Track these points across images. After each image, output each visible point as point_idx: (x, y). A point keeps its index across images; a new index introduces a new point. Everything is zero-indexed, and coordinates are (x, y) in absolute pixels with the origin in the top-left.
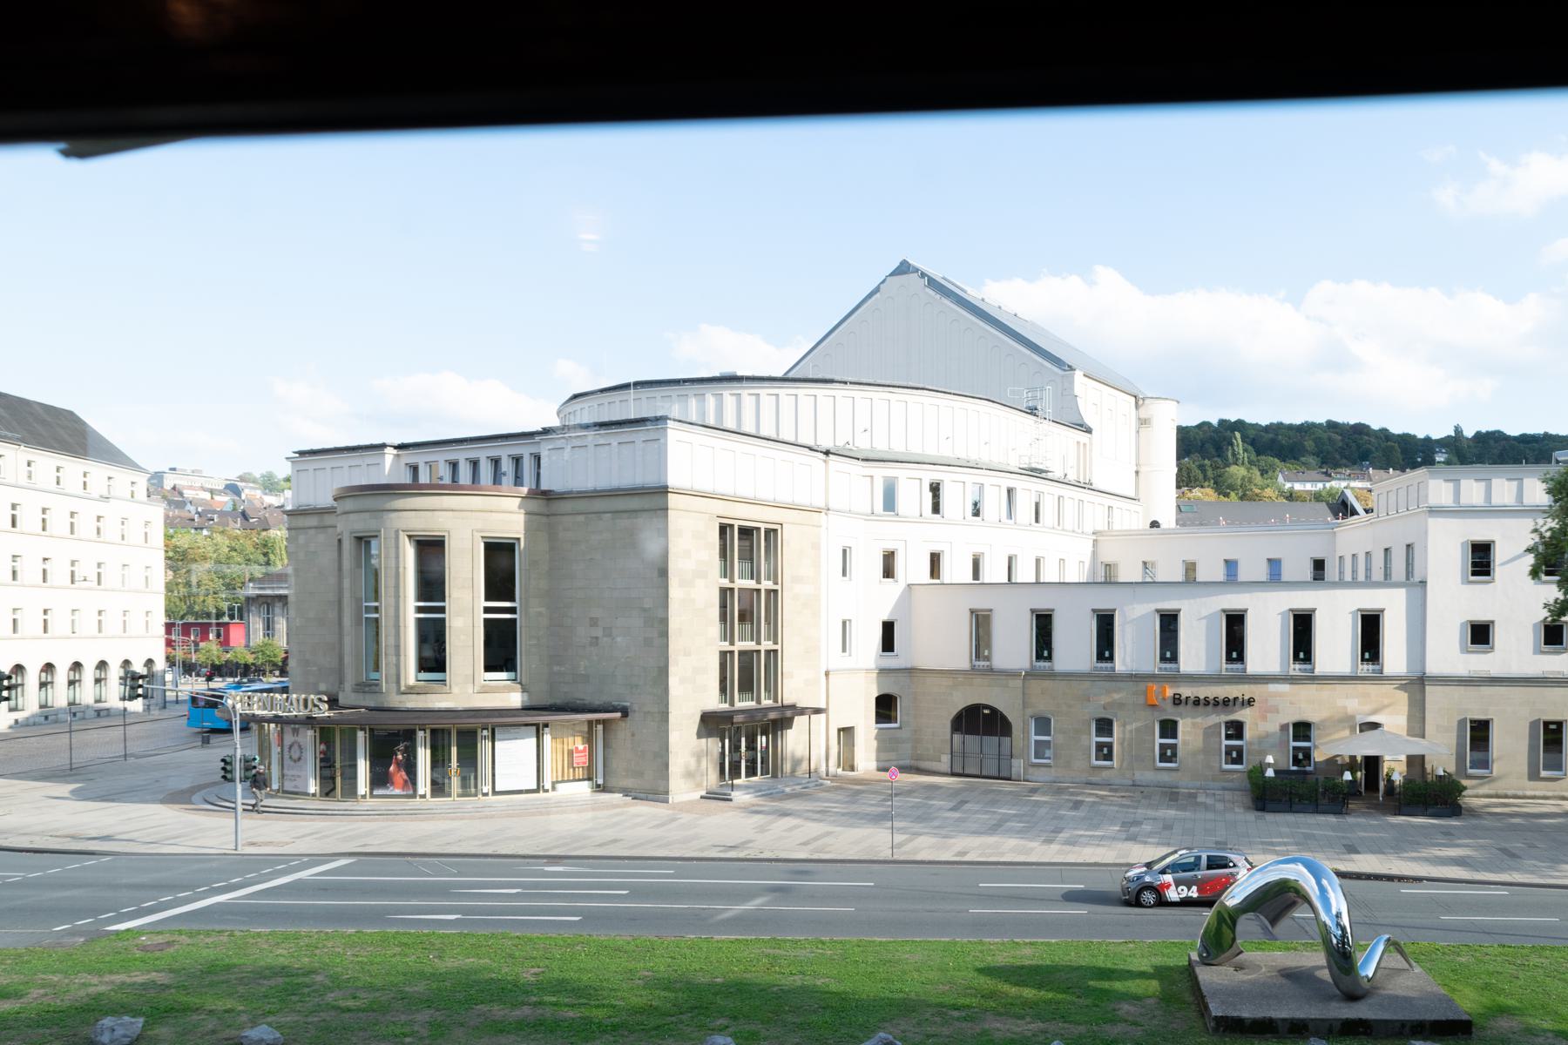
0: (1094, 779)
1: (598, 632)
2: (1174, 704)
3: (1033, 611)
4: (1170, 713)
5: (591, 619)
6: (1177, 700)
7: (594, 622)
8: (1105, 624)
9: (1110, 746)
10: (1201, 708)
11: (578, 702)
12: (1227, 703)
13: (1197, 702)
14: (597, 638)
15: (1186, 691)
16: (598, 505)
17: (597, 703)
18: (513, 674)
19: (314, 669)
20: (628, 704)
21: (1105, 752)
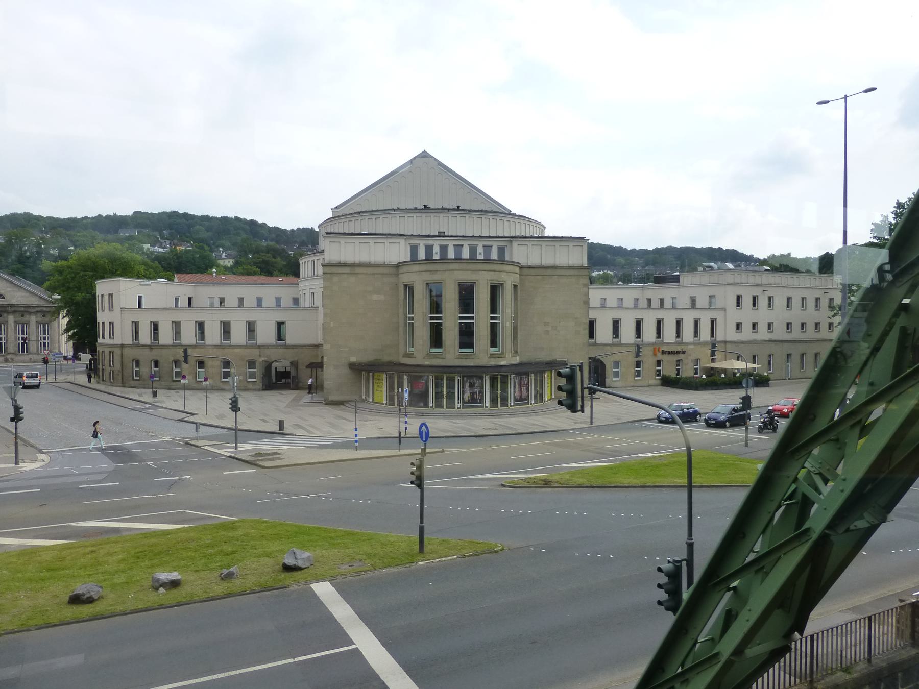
0: (635, 385)
1: (550, 328)
2: (662, 354)
3: (596, 319)
4: (660, 356)
5: (545, 322)
6: (663, 352)
7: (546, 324)
8: (638, 323)
9: (639, 372)
10: (670, 355)
11: (537, 360)
12: (677, 353)
13: (669, 353)
14: (548, 331)
15: (666, 349)
16: (549, 272)
17: (548, 360)
18: (472, 349)
19: (347, 349)
20: (566, 360)
21: (638, 374)
